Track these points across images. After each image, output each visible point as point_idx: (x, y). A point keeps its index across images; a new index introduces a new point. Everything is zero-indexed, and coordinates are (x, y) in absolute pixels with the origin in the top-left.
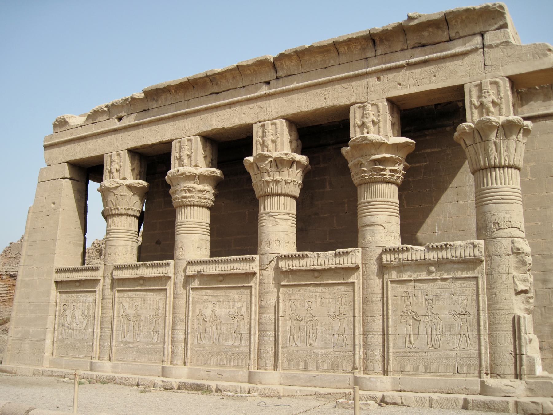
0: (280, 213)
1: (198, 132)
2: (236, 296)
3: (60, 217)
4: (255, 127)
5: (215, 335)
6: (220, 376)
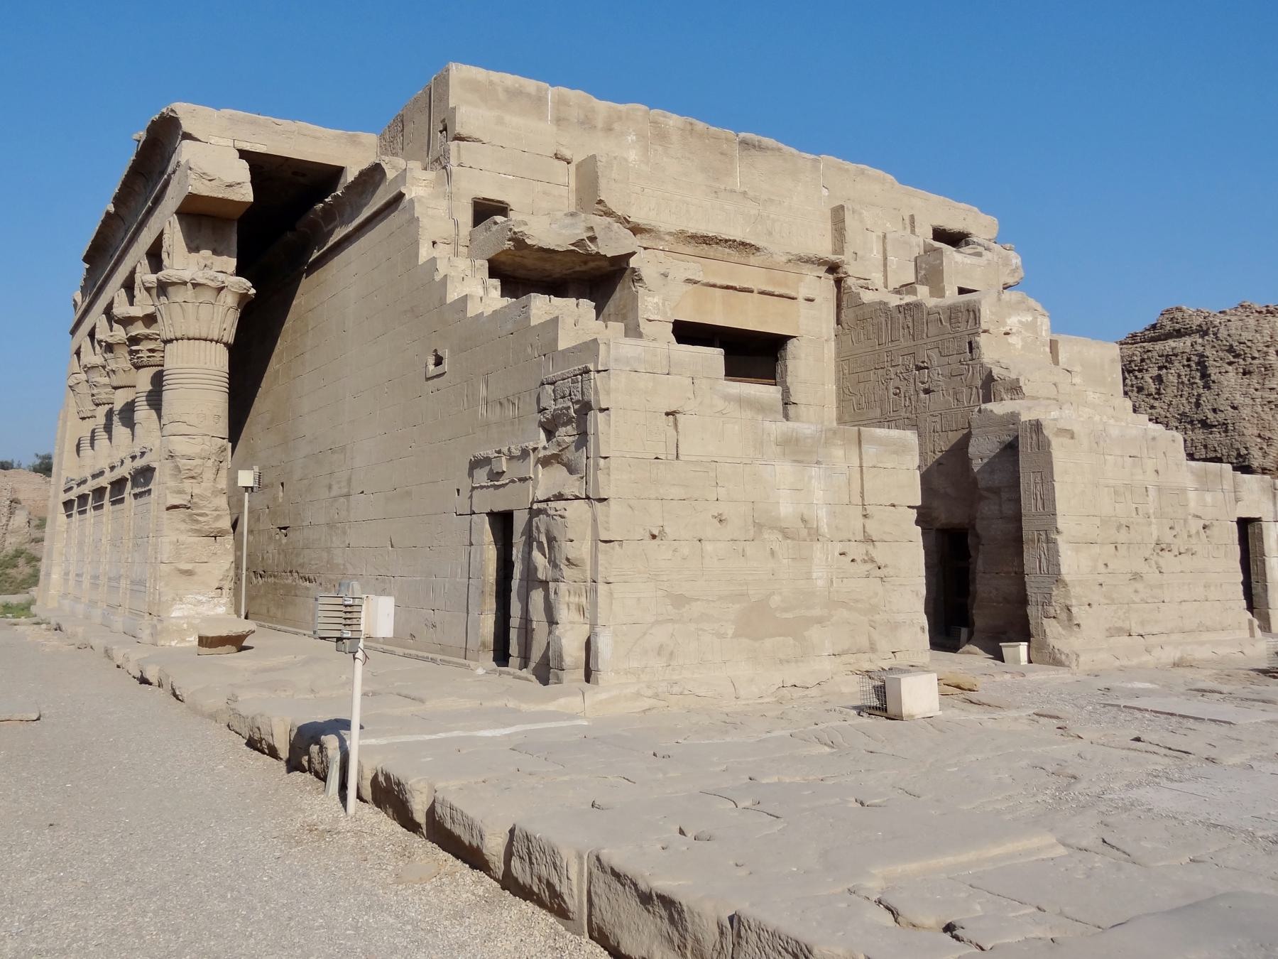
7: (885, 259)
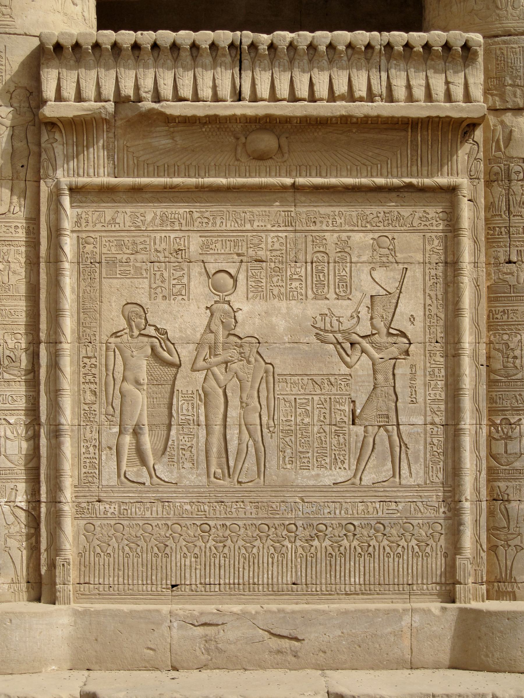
2: (357, 237)
5: (233, 434)
6: (286, 644)
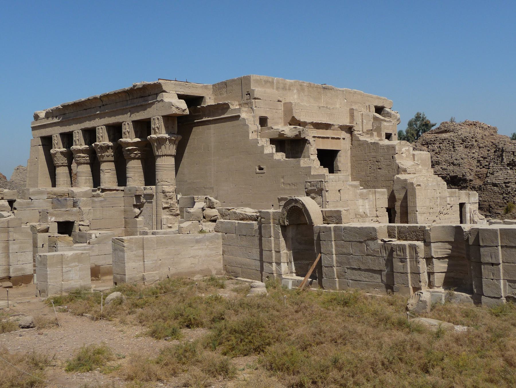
0: (106, 170)
1: (80, 128)
3: (39, 165)
4: (97, 128)
7: (362, 121)
